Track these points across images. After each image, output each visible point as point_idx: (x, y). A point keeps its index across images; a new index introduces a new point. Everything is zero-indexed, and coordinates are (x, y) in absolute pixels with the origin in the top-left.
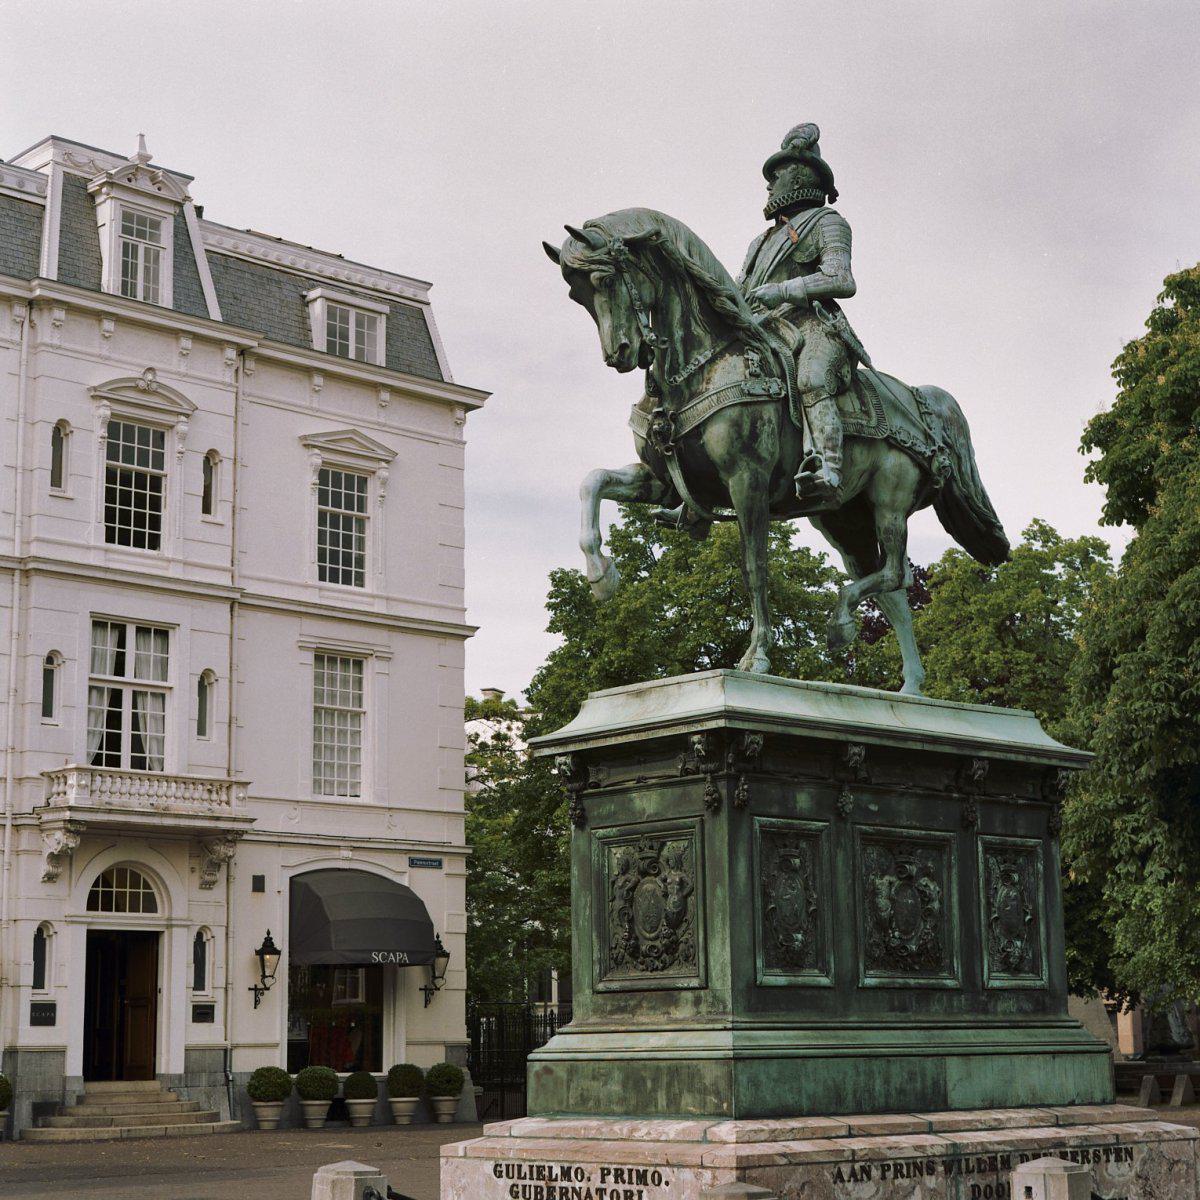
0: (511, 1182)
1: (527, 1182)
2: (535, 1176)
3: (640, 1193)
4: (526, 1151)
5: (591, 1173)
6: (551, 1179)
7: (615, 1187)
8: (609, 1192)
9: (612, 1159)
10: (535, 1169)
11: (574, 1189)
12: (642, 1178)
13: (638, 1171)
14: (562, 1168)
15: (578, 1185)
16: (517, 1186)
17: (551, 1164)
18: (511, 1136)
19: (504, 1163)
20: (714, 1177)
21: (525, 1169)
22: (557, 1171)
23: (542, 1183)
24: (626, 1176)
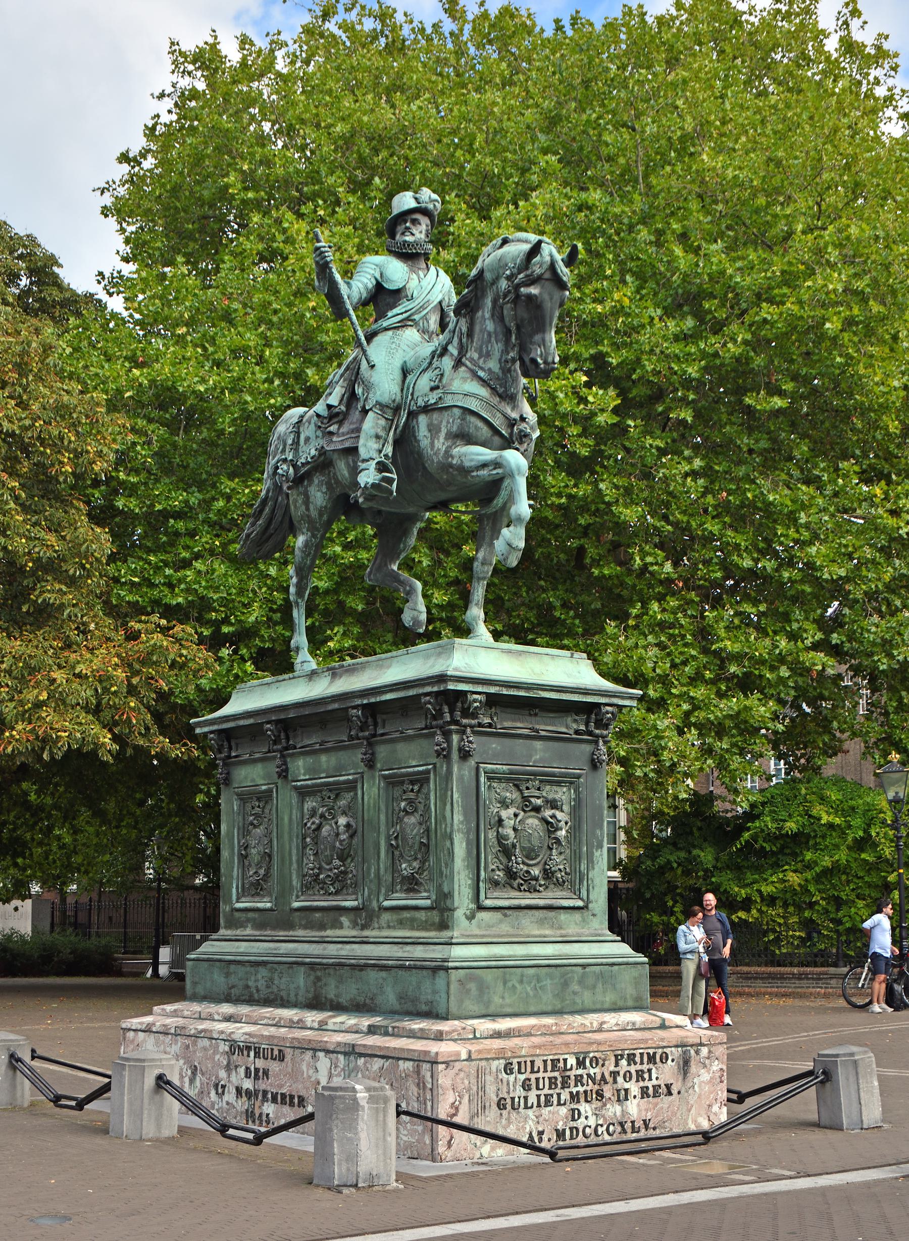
0: (522, 1077)
1: (541, 1075)
2: (549, 1068)
3: (650, 1071)
4: (540, 1047)
5: (604, 1060)
6: (565, 1070)
7: (628, 1068)
8: (622, 1073)
9: (626, 1046)
10: (549, 1063)
11: (589, 1075)
12: (652, 1059)
13: (648, 1054)
14: (578, 1059)
15: (592, 1071)
16: (529, 1080)
17: (566, 1056)
18: (475, 1038)
19: (515, 1061)
20: (710, 1052)
21: (539, 1063)
22: (572, 1061)
23: (556, 1074)
24: (638, 1059)
